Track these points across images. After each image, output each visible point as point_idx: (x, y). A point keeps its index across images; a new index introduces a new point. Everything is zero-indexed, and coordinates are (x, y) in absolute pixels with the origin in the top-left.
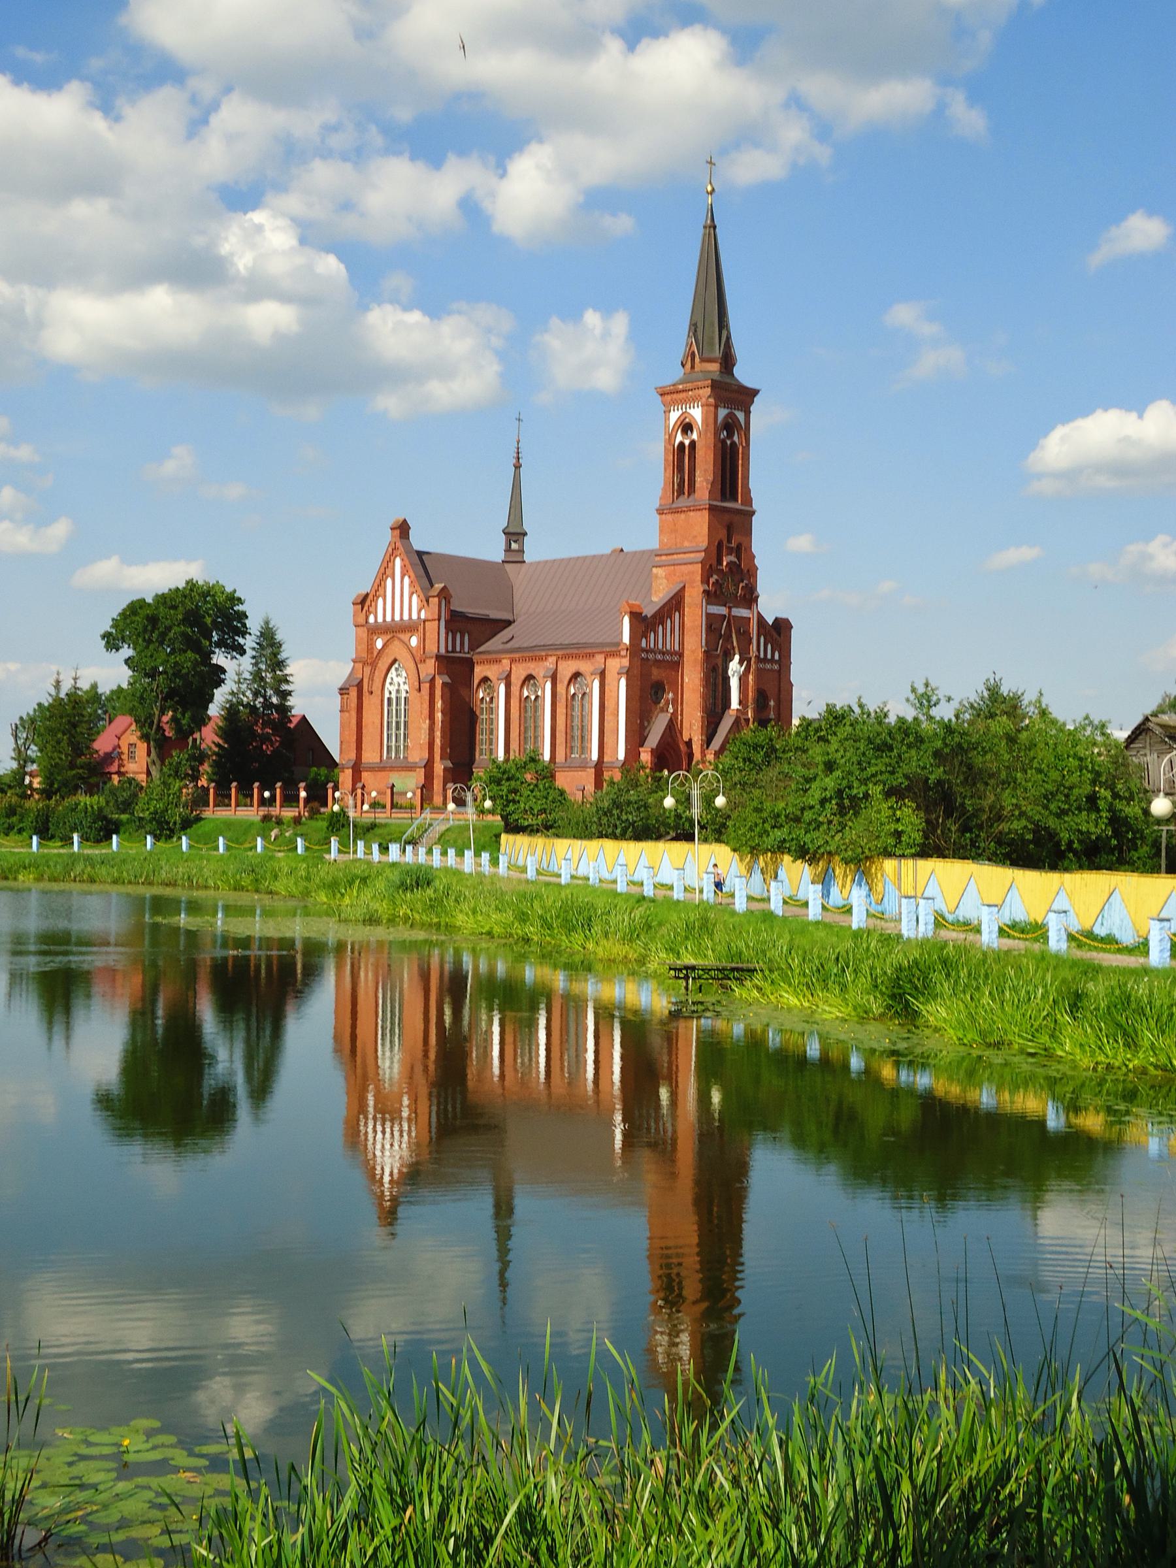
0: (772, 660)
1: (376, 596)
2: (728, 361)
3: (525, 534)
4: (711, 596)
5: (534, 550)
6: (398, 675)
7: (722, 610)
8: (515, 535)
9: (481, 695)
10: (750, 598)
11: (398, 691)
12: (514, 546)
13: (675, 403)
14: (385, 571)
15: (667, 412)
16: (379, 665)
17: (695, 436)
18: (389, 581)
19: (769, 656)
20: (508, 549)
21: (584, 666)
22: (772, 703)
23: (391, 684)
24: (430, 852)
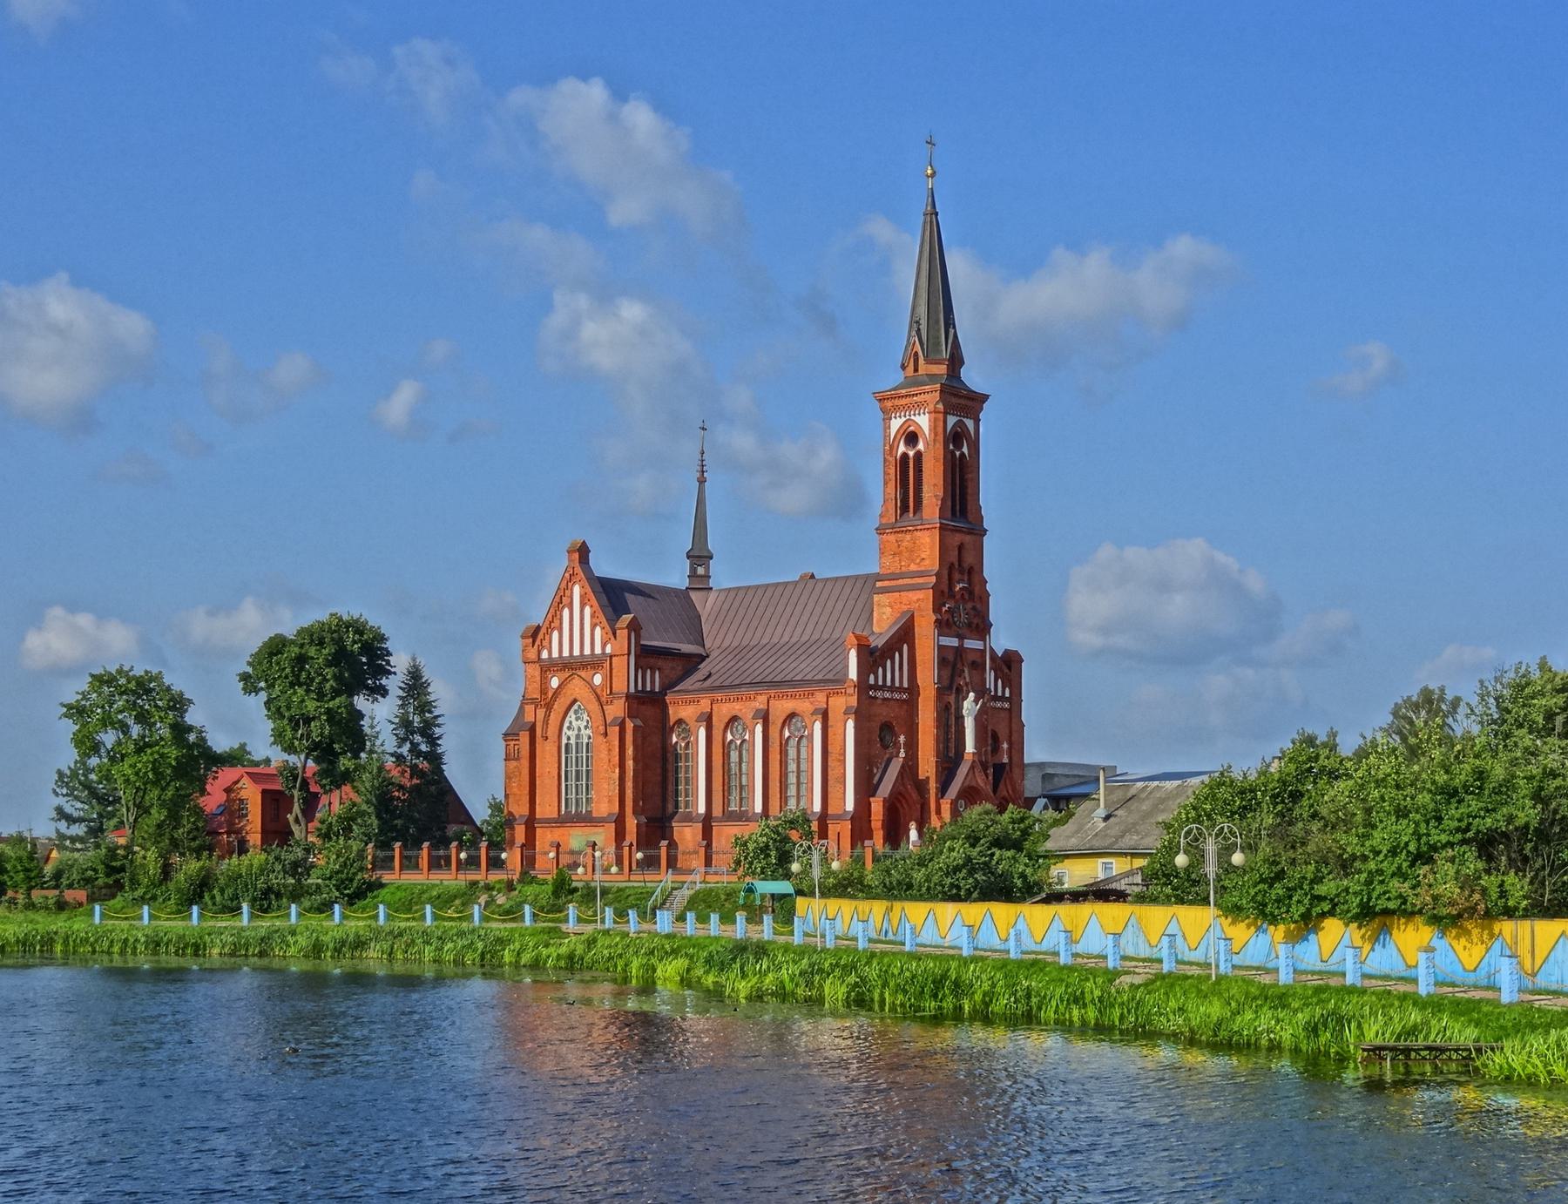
0: (1002, 699)
1: (550, 629)
2: (956, 361)
3: (711, 558)
4: (943, 626)
5: (722, 576)
6: (577, 719)
7: (954, 642)
8: (699, 557)
9: (674, 739)
10: (982, 627)
11: (578, 736)
12: (700, 571)
13: (896, 408)
14: (561, 600)
15: (887, 420)
16: (555, 706)
17: (921, 446)
18: (566, 612)
19: (1000, 694)
20: (693, 575)
21: (803, 706)
22: (1005, 746)
23: (569, 728)
24: (681, 918)
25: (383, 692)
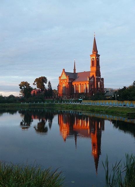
2: (97, 52)
7: (99, 77)
8: (75, 70)
20: (74, 71)
25: (46, 83)
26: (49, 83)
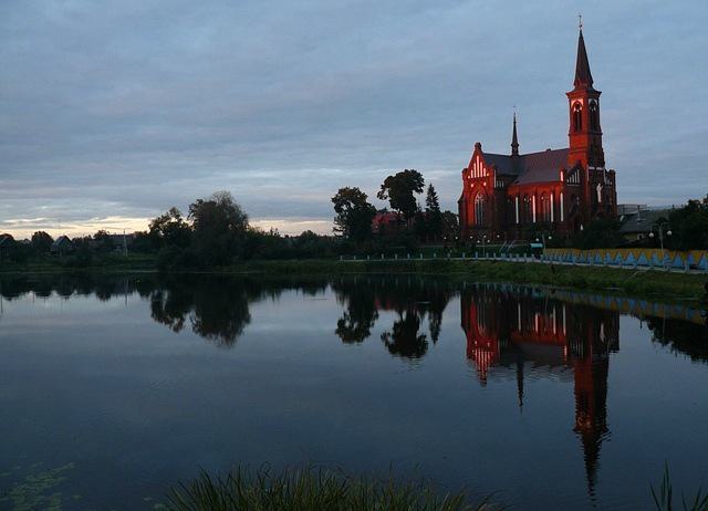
8: (515, 145)
10: (603, 164)
21: (547, 190)
25: (422, 191)
26: (431, 190)
